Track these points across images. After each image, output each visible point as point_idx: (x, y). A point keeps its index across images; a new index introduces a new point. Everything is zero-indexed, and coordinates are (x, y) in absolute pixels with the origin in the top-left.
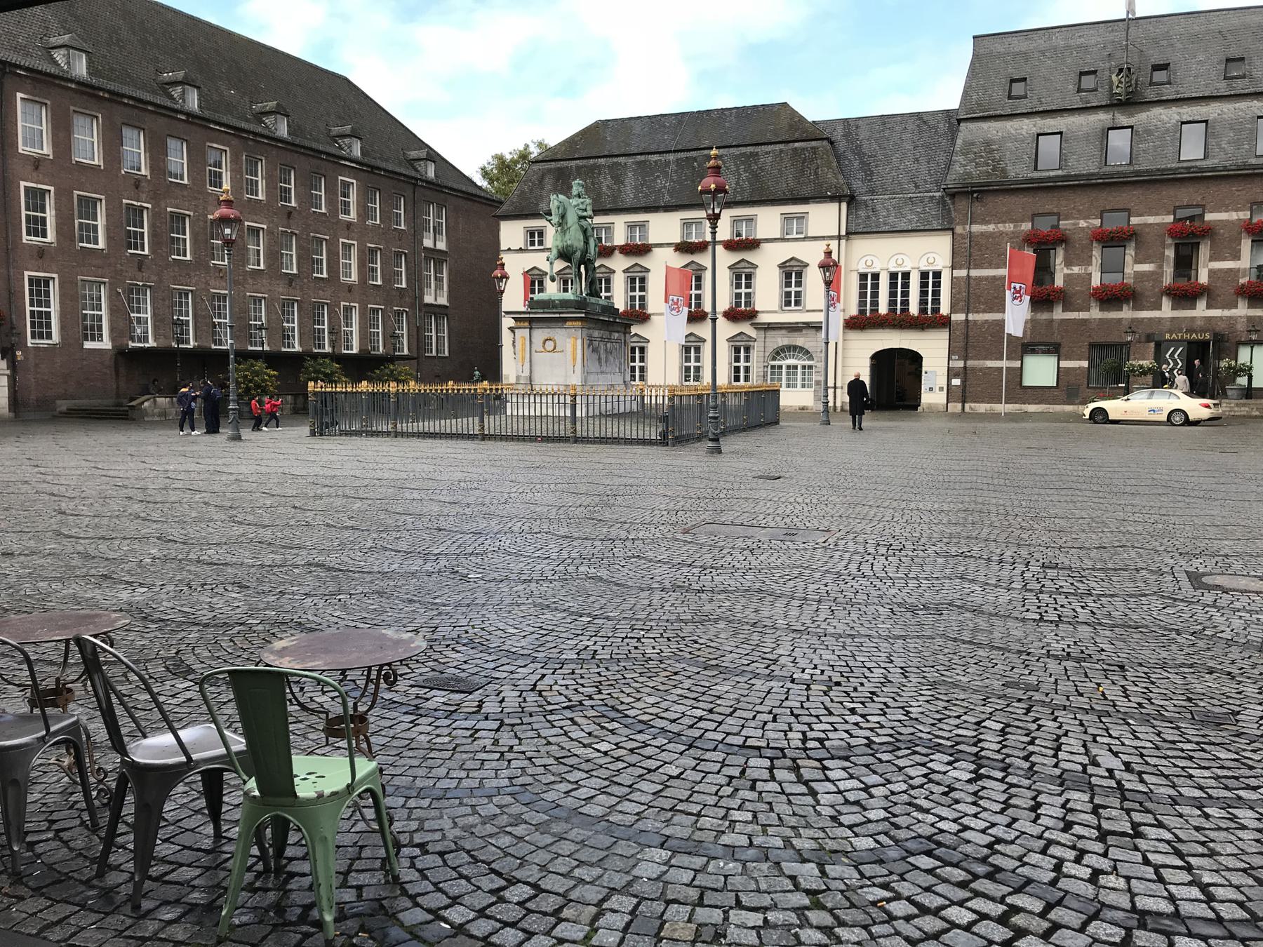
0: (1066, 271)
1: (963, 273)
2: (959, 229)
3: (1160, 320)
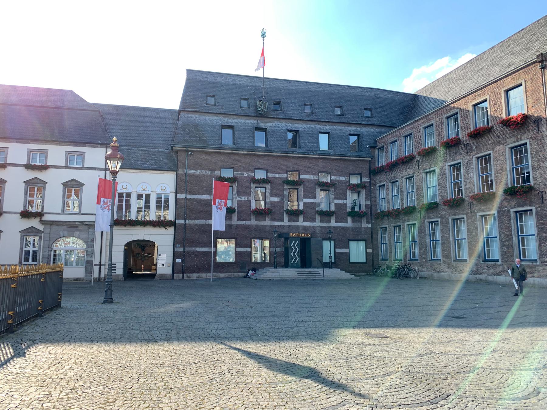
0: (238, 198)
1: (182, 196)
2: (180, 171)
3: (282, 227)
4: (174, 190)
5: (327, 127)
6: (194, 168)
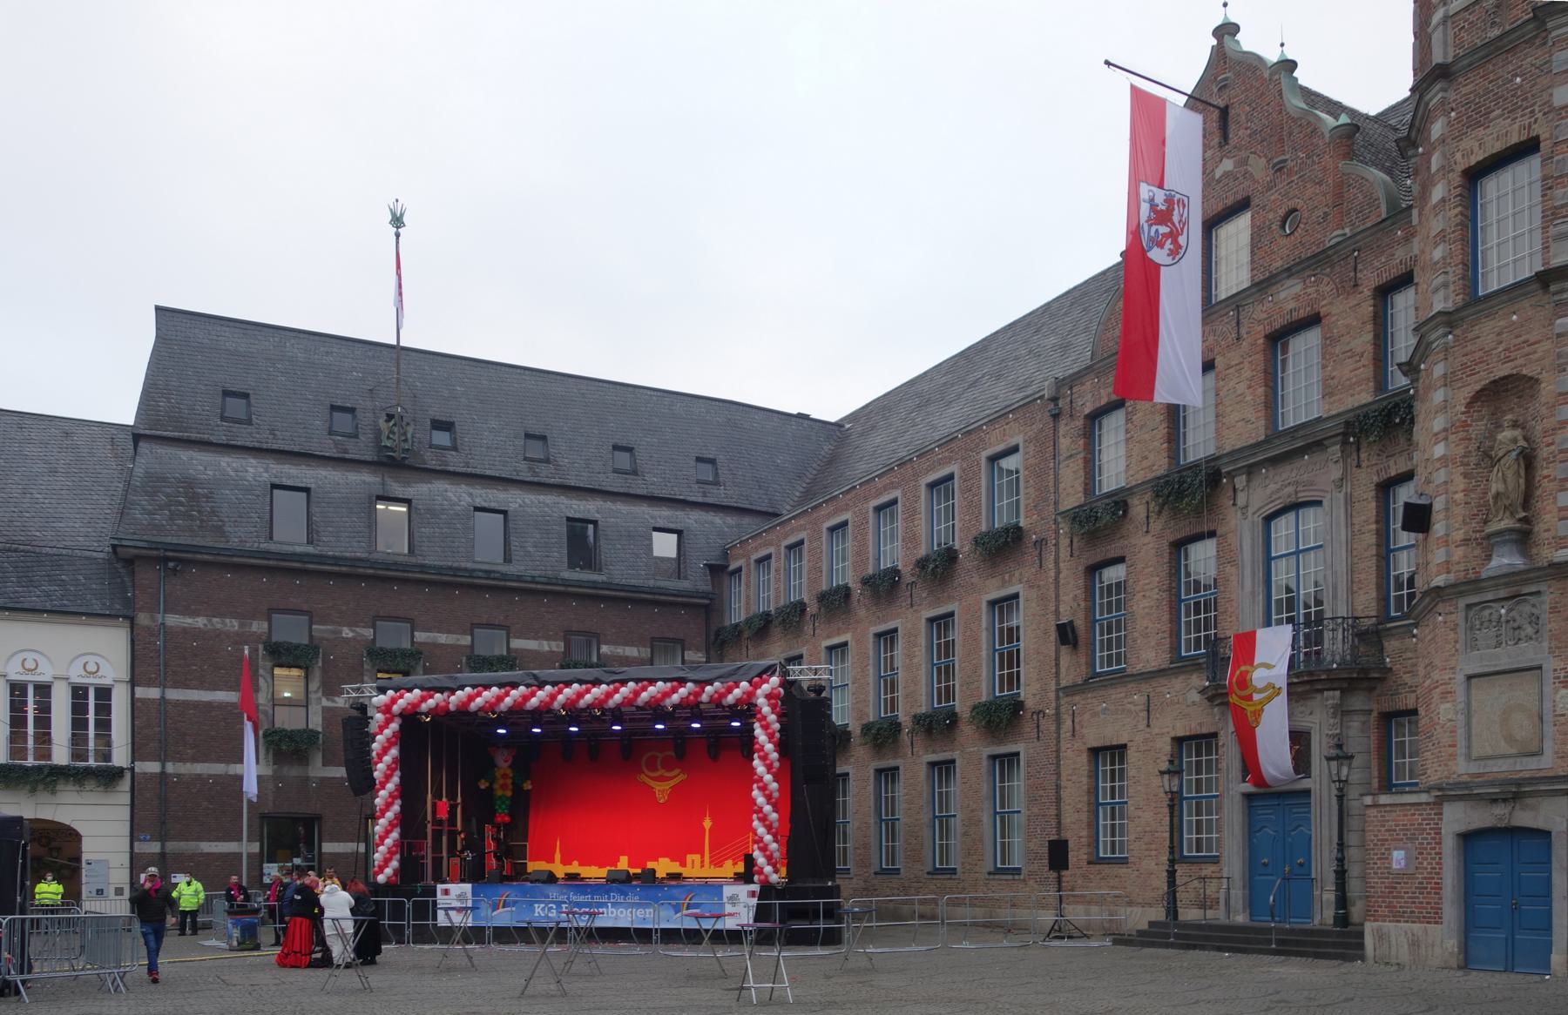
2: (143, 619)
4: (124, 672)
6: (187, 611)
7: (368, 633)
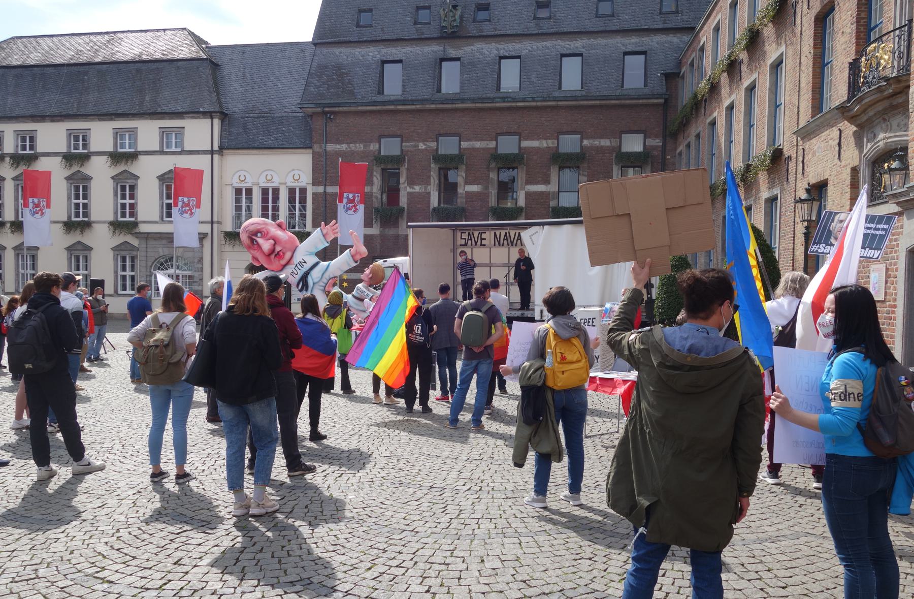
0: (409, 190)
1: (320, 189)
5: (578, 44)
7: (433, 145)
